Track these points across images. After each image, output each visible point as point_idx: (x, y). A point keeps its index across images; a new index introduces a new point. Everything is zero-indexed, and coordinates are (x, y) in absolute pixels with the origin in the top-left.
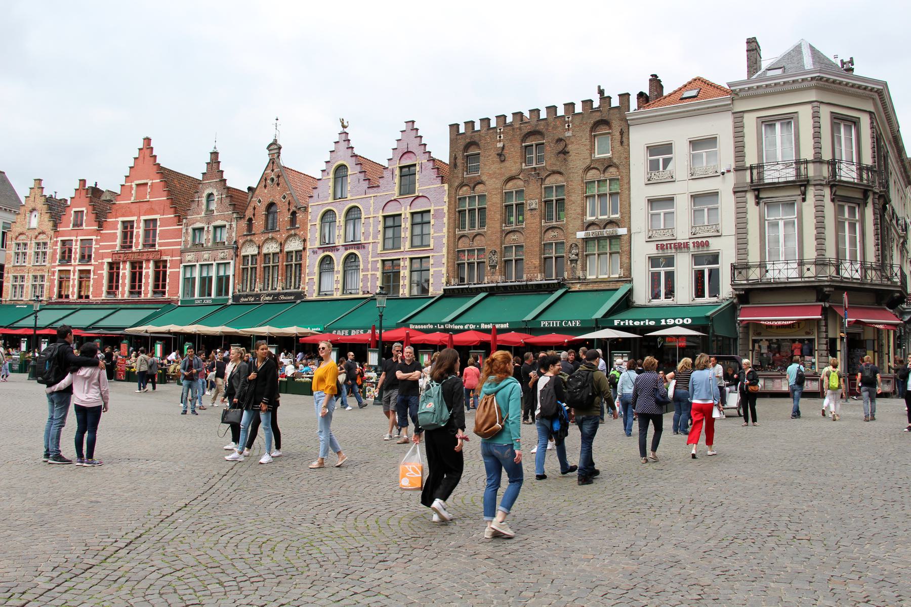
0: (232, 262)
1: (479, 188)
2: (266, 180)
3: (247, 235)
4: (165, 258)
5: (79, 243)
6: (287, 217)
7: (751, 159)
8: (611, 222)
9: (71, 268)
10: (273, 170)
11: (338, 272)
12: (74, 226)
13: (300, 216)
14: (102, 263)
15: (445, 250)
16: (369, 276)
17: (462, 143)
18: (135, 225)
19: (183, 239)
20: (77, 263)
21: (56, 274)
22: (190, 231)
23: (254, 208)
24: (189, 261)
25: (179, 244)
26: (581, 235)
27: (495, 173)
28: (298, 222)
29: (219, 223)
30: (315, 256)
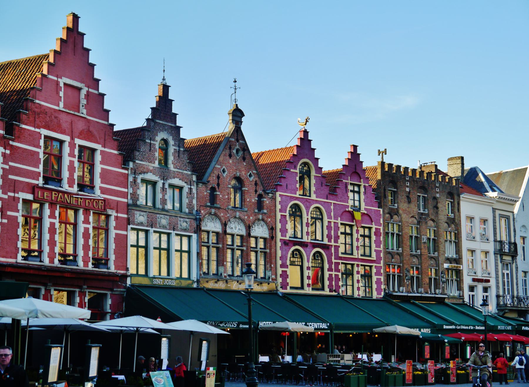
0: (194, 236)
1: (395, 217)
2: (230, 148)
3: (211, 207)
4: (110, 212)
6: (254, 199)
10: (238, 140)
11: (308, 268)
13: (266, 201)
16: (334, 276)
18: (66, 149)
19: (131, 191)
23: (218, 177)
24: (141, 224)
25: (125, 195)
26: (446, 266)
27: (406, 210)
28: (265, 207)
29: (176, 181)
30: (286, 248)
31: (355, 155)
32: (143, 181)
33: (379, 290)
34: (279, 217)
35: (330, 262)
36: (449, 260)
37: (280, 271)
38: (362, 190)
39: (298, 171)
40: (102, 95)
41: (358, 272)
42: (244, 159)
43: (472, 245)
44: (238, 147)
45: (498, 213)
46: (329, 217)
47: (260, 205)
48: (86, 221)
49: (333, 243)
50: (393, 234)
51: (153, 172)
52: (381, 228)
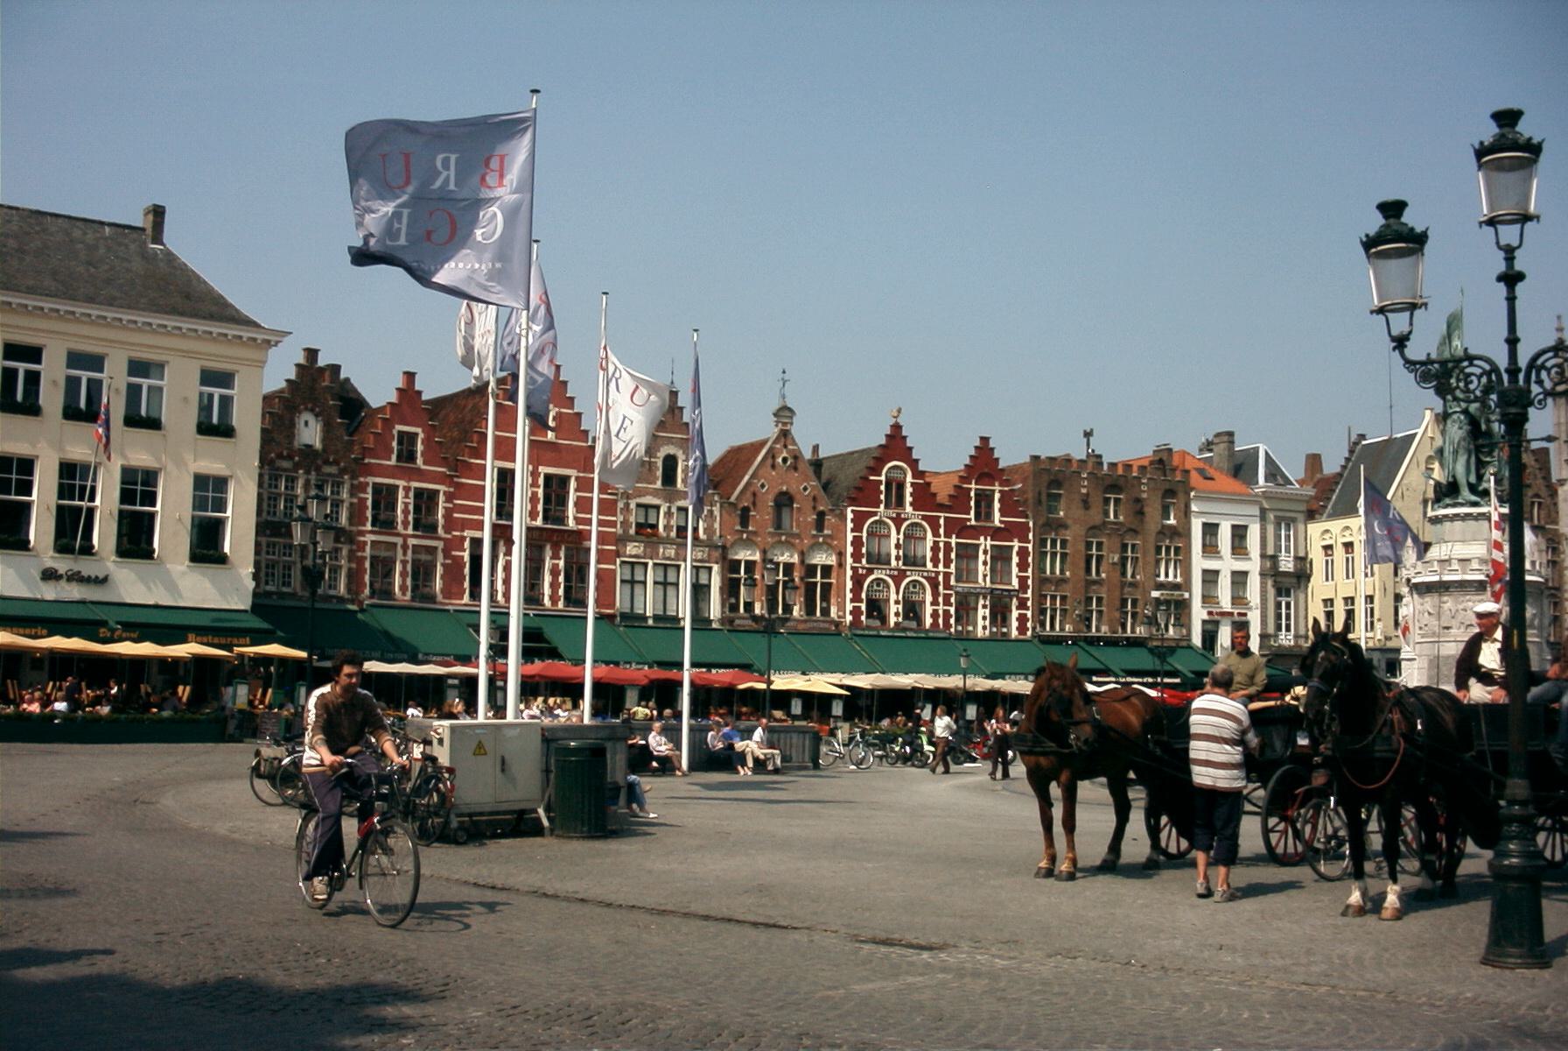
0: (716, 568)
2: (774, 457)
5: (411, 494)
7: (1270, 551)
8: (1176, 587)
9: (399, 541)
11: (897, 602)
12: (399, 458)
13: (830, 519)
14: (464, 538)
15: (1029, 594)
17: (1046, 478)
19: (621, 518)
20: (410, 531)
21: (368, 548)
22: (633, 506)
23: (754, 494)
26: (1155, 594)
31: (984, 451)
32: (638, 505)
33: (1022, 629)
34: (850, 537)
35: (935, 594)
36: (1160, 586)
37: (849, 607)
38: (997, 496)
39: (883, 478)
40: (579, 415)
41: (984, 607)
42: (796, 469)
43: (1212, 564)
44: (785, 454)
45: (1271, 516)
46: (936, 534)
47: (820, 524)
48: (555, 556)
49: (941, 568)
50: (1054, 555)
51: (655, 493)
52: (1030, 546)
